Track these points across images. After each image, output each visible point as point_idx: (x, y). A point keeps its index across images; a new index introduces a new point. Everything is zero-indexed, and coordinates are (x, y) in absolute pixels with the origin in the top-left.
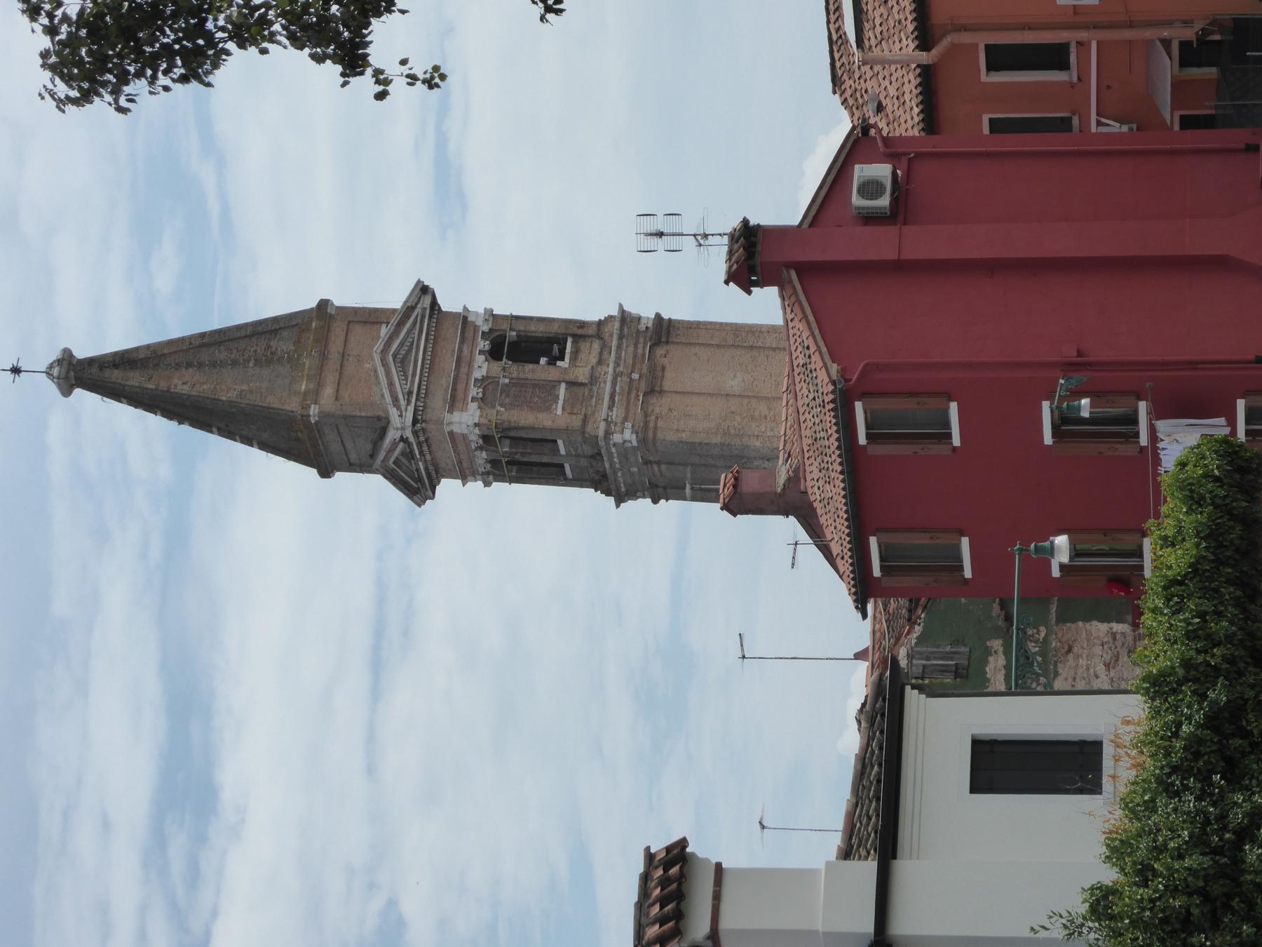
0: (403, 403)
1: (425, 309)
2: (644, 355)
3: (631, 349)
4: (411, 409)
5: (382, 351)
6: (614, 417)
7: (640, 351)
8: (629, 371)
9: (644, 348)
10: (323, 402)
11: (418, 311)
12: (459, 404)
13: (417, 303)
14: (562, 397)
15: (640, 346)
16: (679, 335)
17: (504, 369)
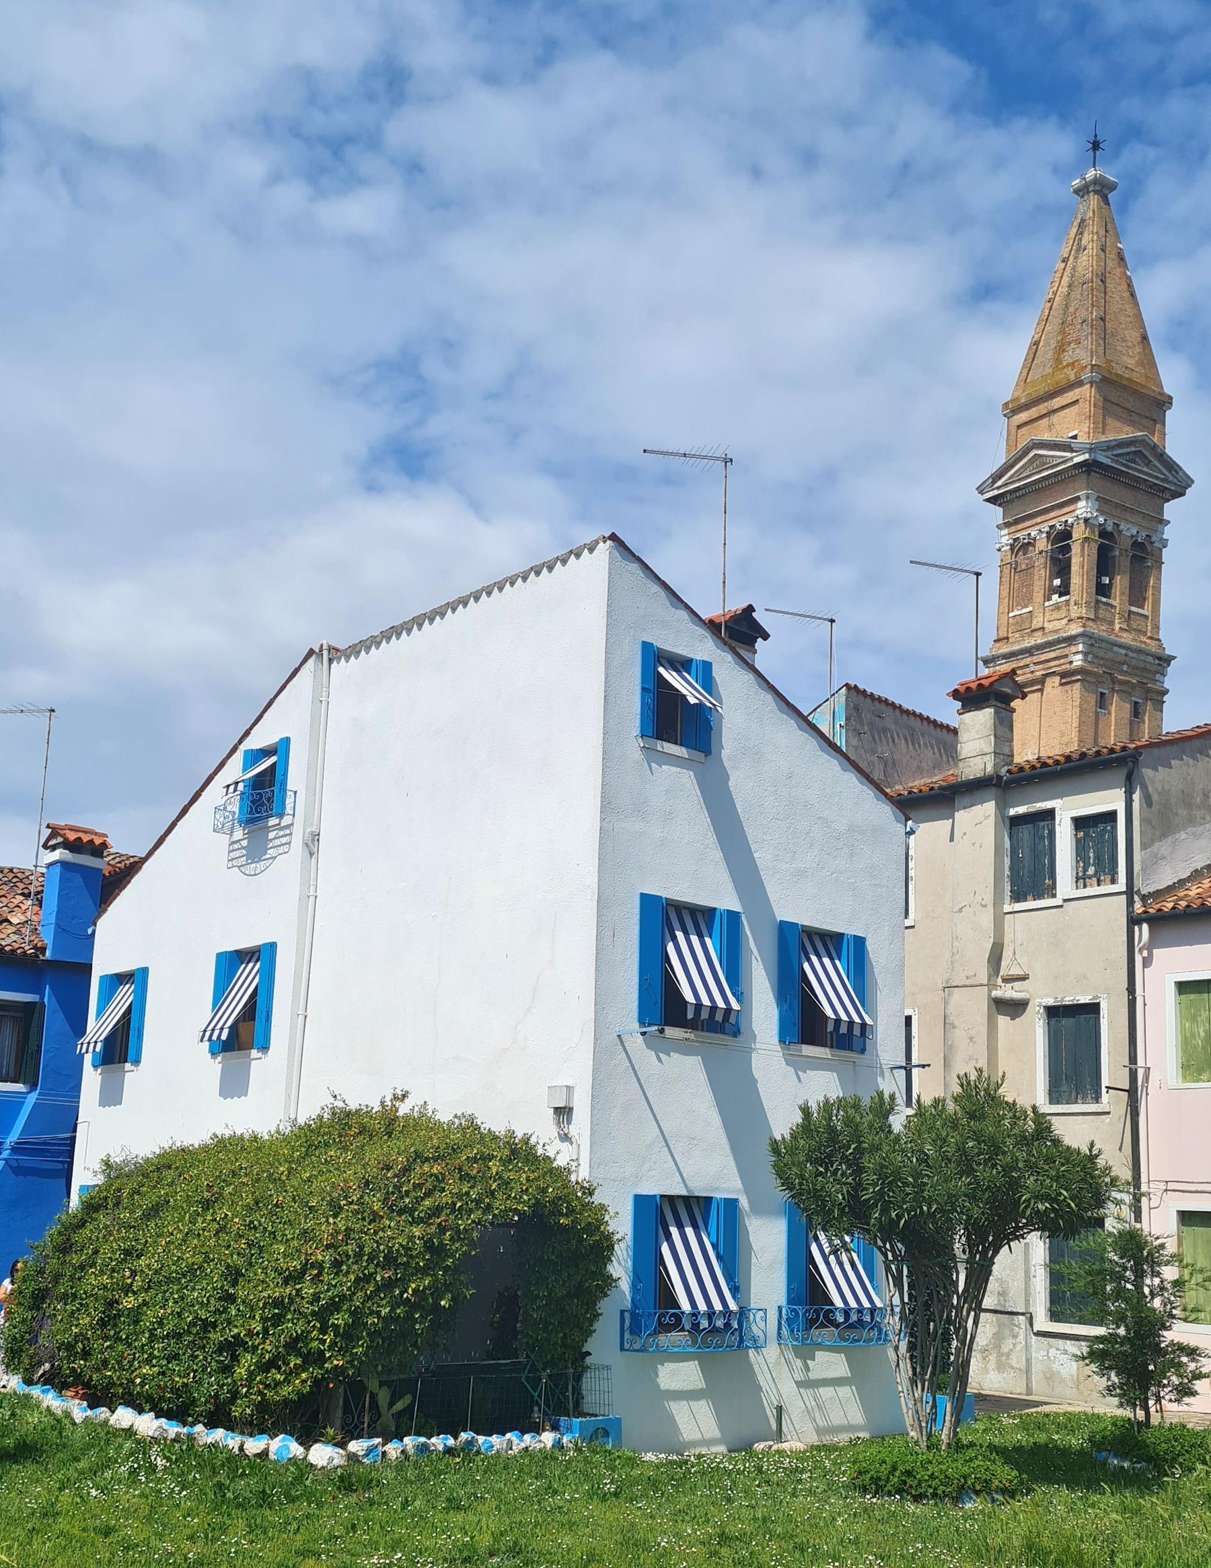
0: (999, 483)
1: (1071, 459)
2: (1050, 668)
3: (1052, 655)
4: (996, 492)
5: (1035, 444)
6: (998, 662)
7: (1052, 664)
8: (1035, 661)
9: (1056, 666)
10: (1015, 417)
11: (1068, 455)
12: (1013, 529)
13: (1076, 451)
14: (1025, 611)
15: (1057, 662)
16: (1067, 693)
17: (1041, 552)
